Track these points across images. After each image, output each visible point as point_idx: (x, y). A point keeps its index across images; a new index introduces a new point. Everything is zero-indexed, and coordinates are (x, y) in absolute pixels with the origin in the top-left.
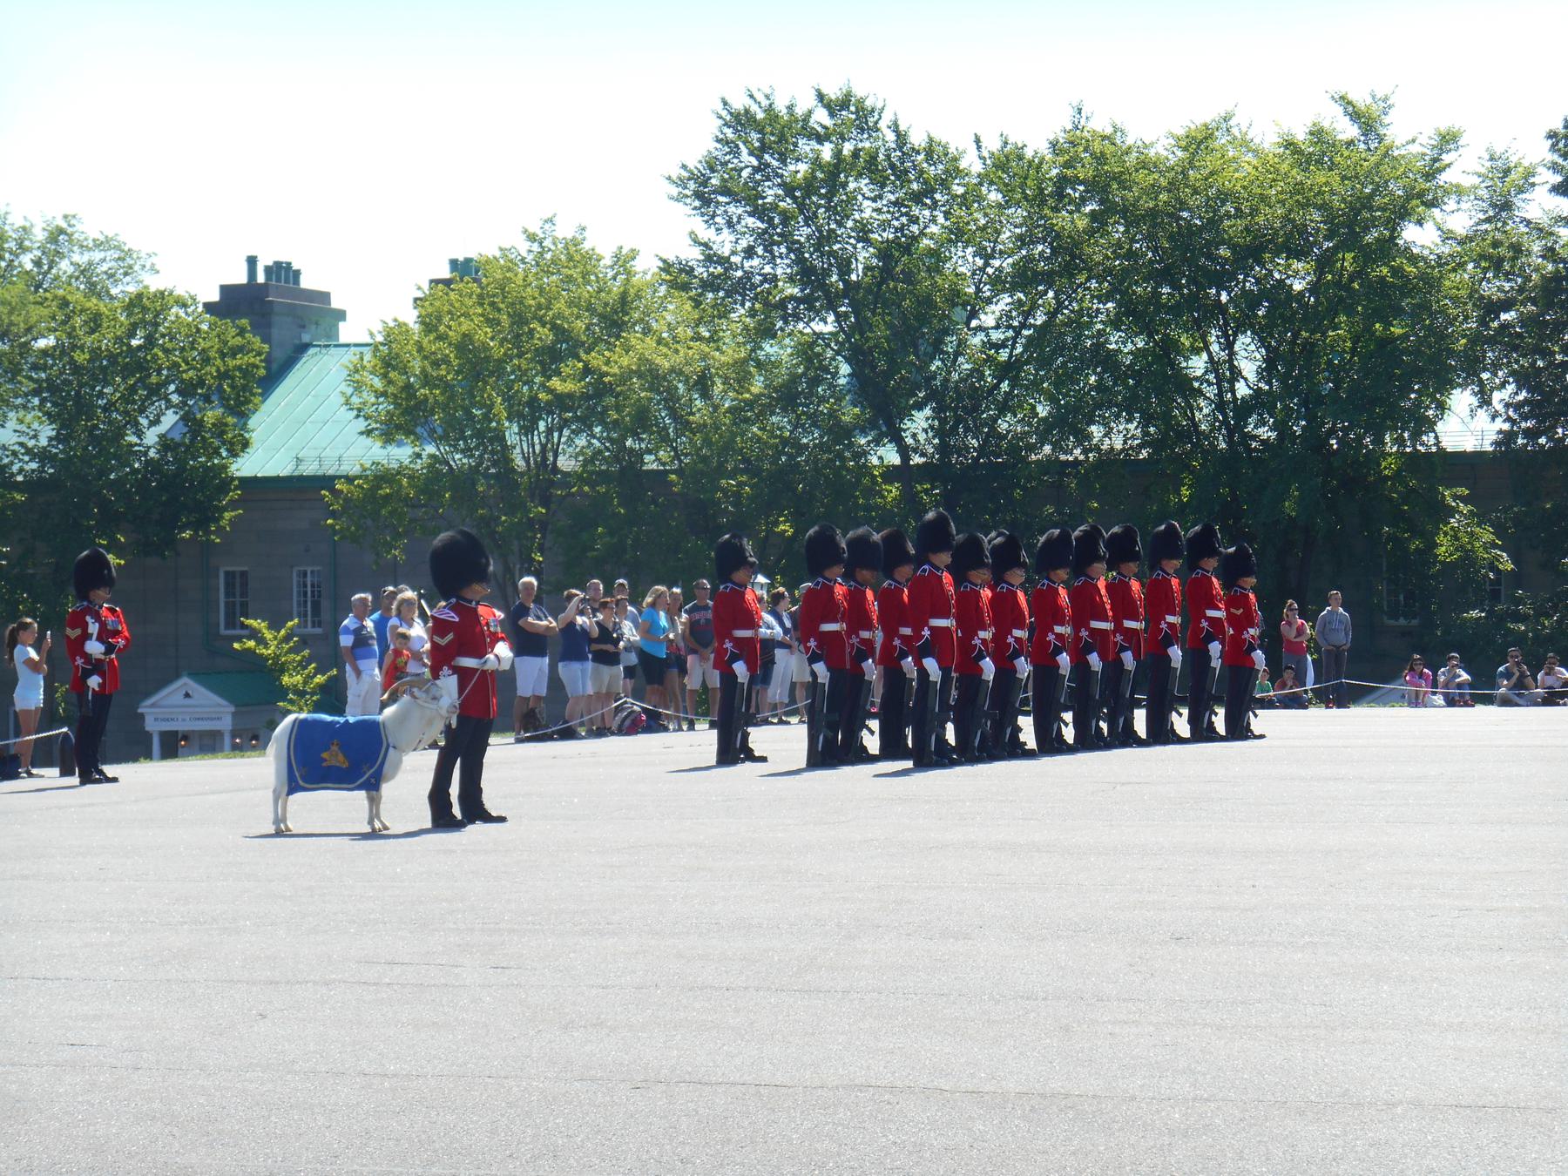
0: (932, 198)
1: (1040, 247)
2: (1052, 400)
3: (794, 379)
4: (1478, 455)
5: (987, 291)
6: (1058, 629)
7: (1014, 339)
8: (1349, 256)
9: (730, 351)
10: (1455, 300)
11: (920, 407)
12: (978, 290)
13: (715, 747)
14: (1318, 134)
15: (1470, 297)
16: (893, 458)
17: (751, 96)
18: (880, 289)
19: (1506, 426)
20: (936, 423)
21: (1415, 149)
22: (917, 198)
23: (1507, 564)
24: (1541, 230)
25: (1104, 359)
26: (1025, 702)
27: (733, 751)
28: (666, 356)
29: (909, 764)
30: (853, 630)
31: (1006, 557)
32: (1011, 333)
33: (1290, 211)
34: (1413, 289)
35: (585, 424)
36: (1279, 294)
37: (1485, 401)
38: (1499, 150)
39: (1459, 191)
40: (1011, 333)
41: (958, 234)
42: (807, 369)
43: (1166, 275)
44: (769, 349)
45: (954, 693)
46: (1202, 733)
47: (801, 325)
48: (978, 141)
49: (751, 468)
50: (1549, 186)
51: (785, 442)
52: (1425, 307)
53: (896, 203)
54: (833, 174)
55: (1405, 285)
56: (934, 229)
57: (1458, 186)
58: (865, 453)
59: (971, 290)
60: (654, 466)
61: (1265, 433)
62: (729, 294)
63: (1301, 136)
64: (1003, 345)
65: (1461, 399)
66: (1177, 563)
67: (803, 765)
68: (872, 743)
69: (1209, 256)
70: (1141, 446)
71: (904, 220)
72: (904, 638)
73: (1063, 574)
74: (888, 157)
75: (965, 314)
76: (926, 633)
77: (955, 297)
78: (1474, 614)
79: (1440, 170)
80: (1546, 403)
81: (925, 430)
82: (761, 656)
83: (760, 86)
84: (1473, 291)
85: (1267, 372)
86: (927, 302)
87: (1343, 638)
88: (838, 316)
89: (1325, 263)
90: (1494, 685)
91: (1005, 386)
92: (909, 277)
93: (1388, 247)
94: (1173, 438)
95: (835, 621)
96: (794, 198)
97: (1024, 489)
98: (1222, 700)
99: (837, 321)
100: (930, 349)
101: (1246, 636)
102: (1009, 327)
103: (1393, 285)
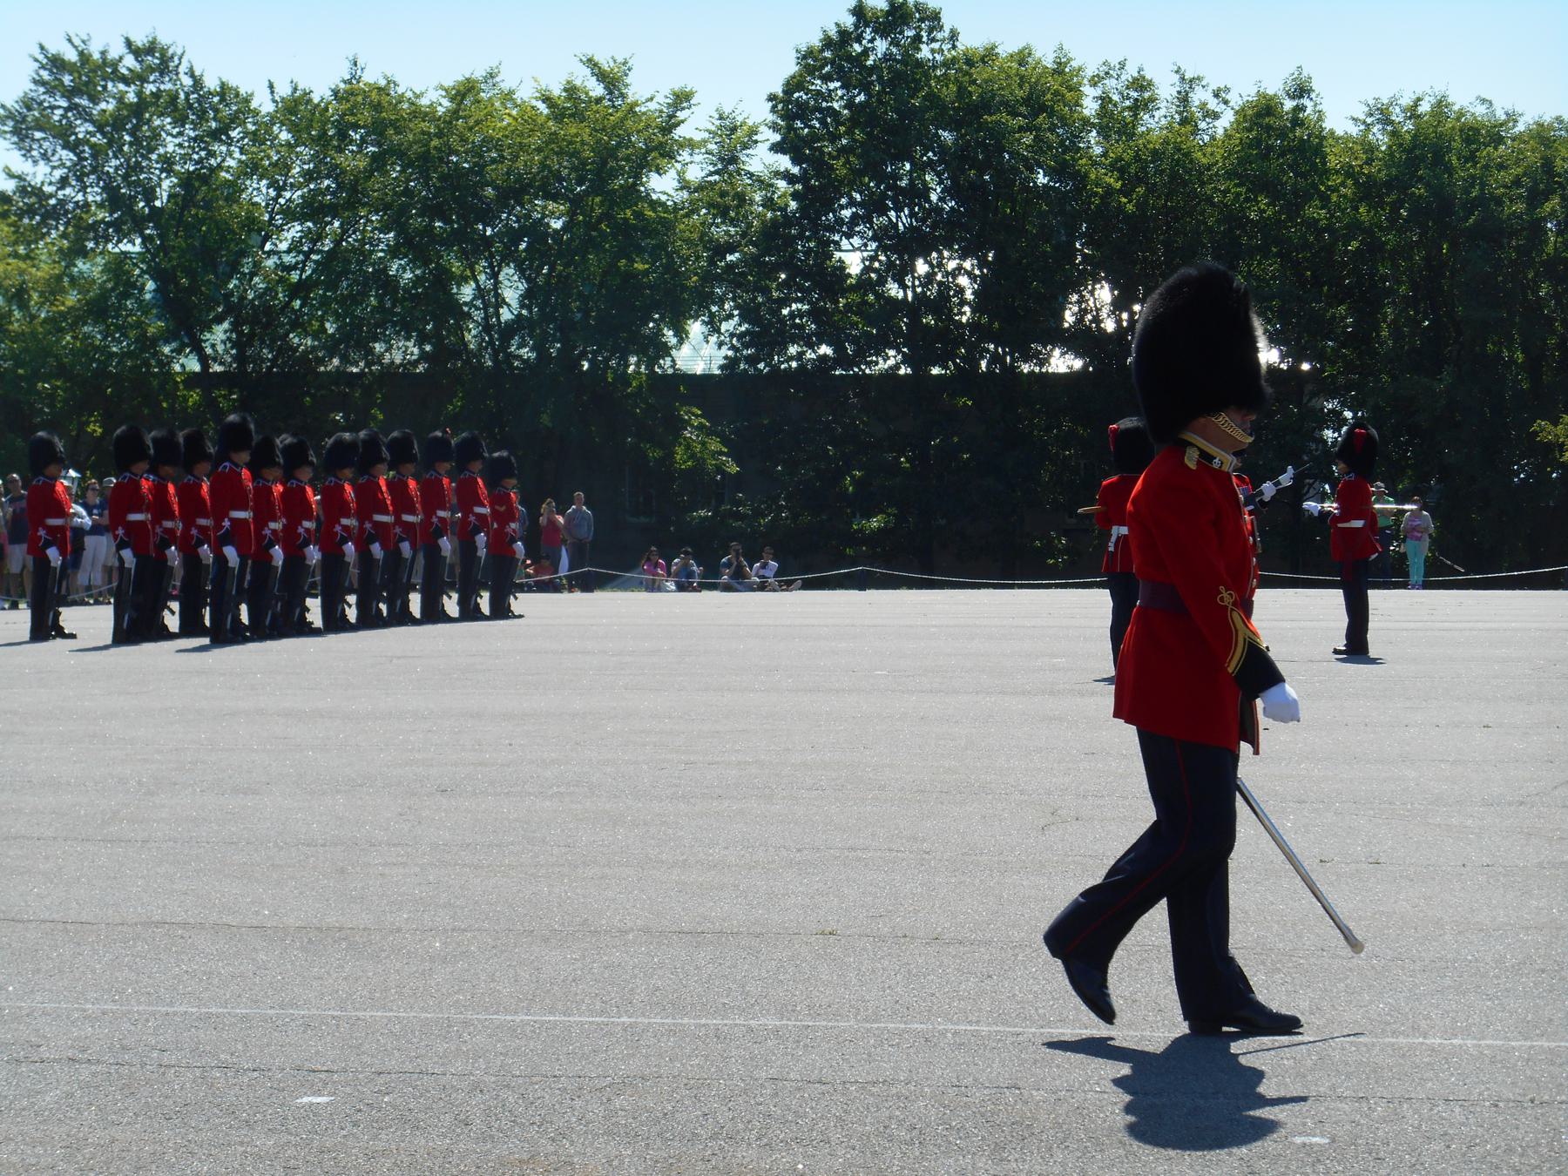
0: (229, 137)
1: (326, 182)
2: (338, 317)
3: (104, 294)
4: (706, 378)
5: (279, 220)
6: (345, 521)
7: (304, 262)
8: (598, 199)
9: (44, 268)
10: (687, 241)
11: (219, 320)
12: (272, 218)
13: (28, 625)
14: (571, 90)
15: (701, 239)
16: (197, 368)
17: (70, 40)
18: (182, 214)
19: (730, 353)
21: (652, 106)
22: (215, 135)
23: (734, 469)
24: (762, 182)
25: (388, 284)
26: (313, 585)
27: (45, 628)
29: (206, 641)
30: (156, 521)
31: (296, 456)
32: (301, 257)
33: (546, 158)
34: (656, 227)
36: (536, 231)
38: (727, 110)
39: (691, 144)
40: (301, 257)
41: (252, 168)
42: (117, 284)
43: (433, 210)
44: (81, 265)
45: (248, 577)
46: (470, 613)
47: (110, 246)
48: (271, 86)
49: (62, 371)
50: (768, 144)
51: (97, 349)
52: (662, 246)
53: (195, 139)
54: (139, 109)
55: (647, 228)
56: (231, 163)
57: (691, 140)
58: (169, 363)
59: (266, 217)
61: (524, 352)
62: (45, 218)
63: (557, 91)
64: (294, 267)
66: (447, 466)
67: (109, 641)
68: (172, 622)
69: (475, 195)
70: (416, 362)
71: (203, 154)
72: (203, 530)
73: (348, 473)
74: (187, 99)
75: (259, 239)
76: (226, 523)
77: (251, 224)
78: (702, 513)
79: (678, 124)
80: (766, 334)
81: (224, 342)
82: (72, 543)
83: (79, 31)
84: (703, 234)
85: (528, 297)
86: (223, 229)
87: (586, 533)
88: (146, 240)
89: (576, 203)
90: (718, 575)
91: (297, 304)
92: (208, 205)
93: (632, 194)
94: (445, 352)
95: (140, 511)
96: (104, 134)
97: (312, 396)
98: (488, 584)
99: (143, 243)
100: (228, 269)
101: (507, 529)
102: (299, 252)
103: (635, 228)
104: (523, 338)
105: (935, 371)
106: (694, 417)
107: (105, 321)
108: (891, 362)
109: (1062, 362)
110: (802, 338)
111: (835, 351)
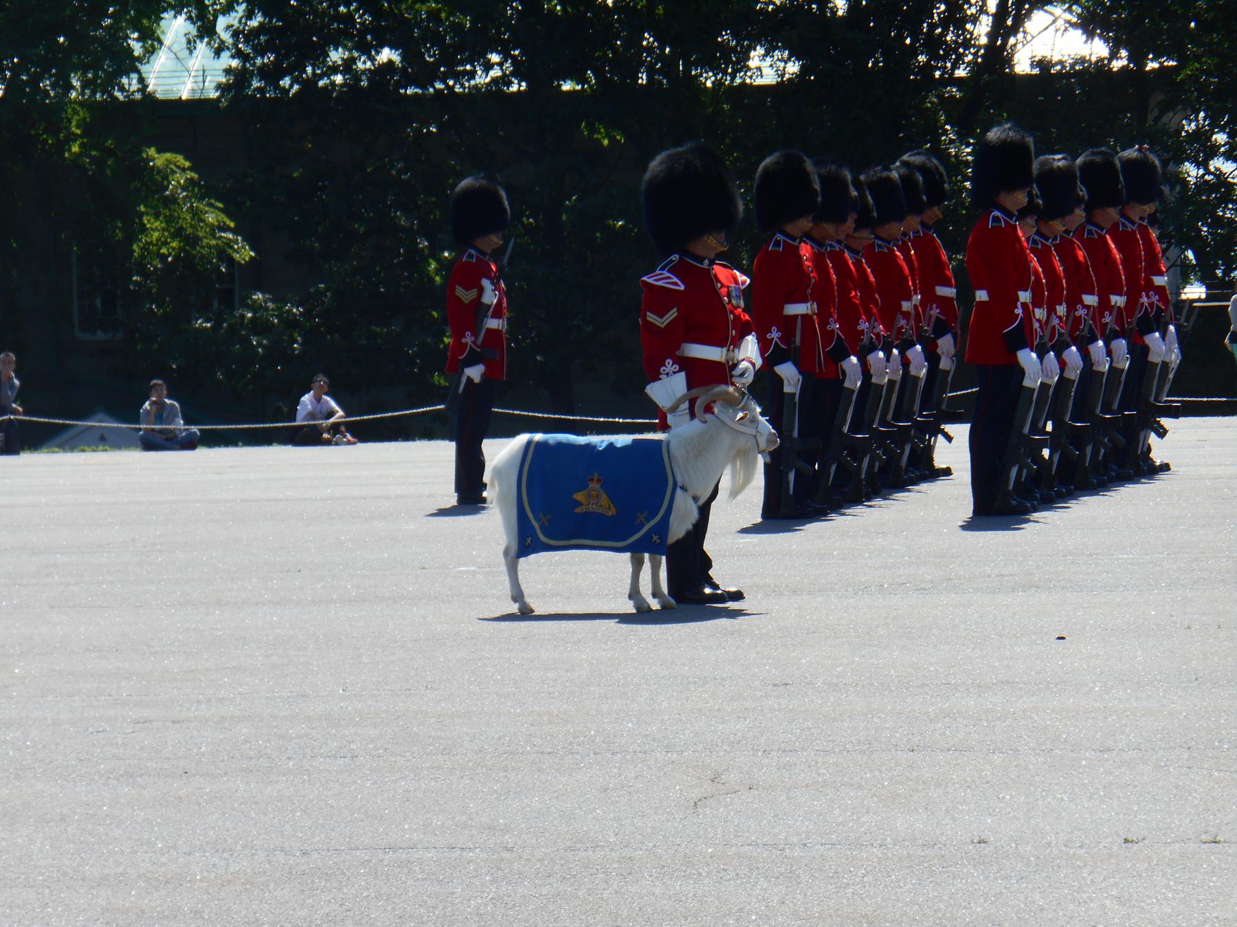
19: (235, 63)
37: (206, 30)
65: (175, 27)
105: (567, 86)
106: (172, 166)
108: (496, 72)
109: (766, 68)
110: (351, 37)
111: (404, 58)
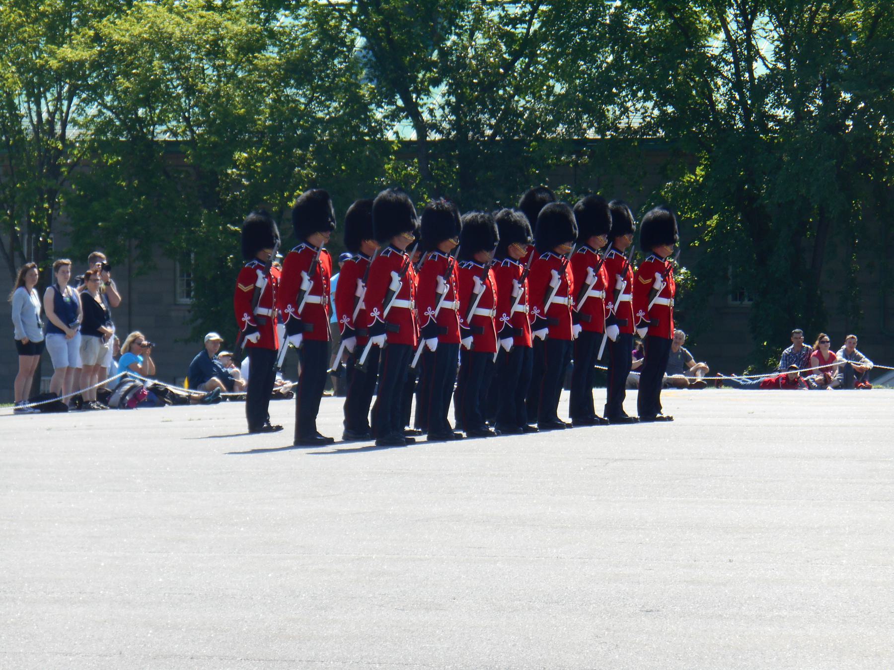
7: (532, 13)
11: (436, 83)
16: (411, 135)
20: (453, 99)
28: (178, 24)
35: (96, 93)
60: (167, 137)
61: (780, 113)
85: (785, 50)
104: (778, 95)
107: (310, 82)
